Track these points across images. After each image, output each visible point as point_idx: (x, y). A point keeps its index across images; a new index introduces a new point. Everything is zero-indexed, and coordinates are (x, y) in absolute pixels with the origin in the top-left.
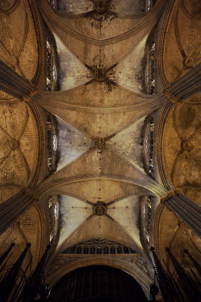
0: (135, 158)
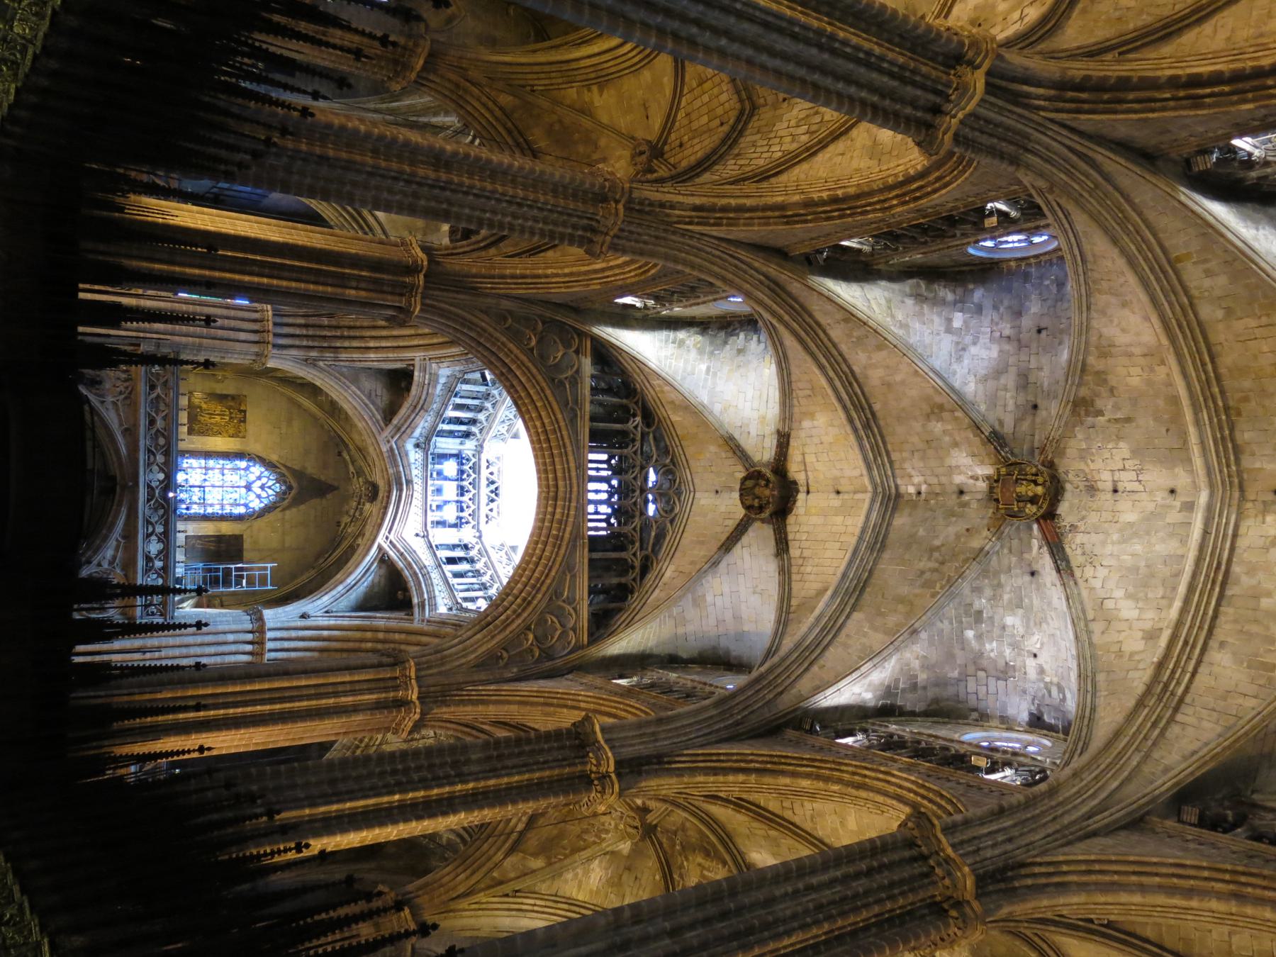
0: (955, 674)
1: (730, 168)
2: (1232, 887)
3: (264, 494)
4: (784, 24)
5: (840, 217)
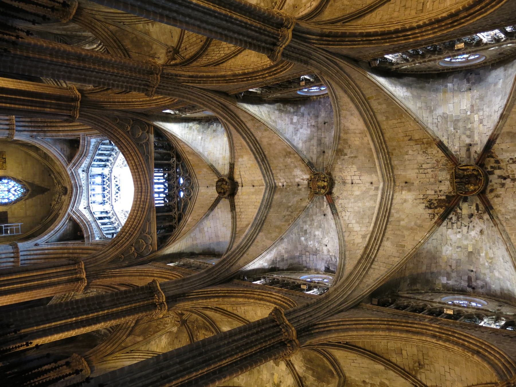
0: (298, 254)
1: (204, 60)
2: (387, 326)
3: (16, 194)
4: (211, 12)
5: (247, 80)
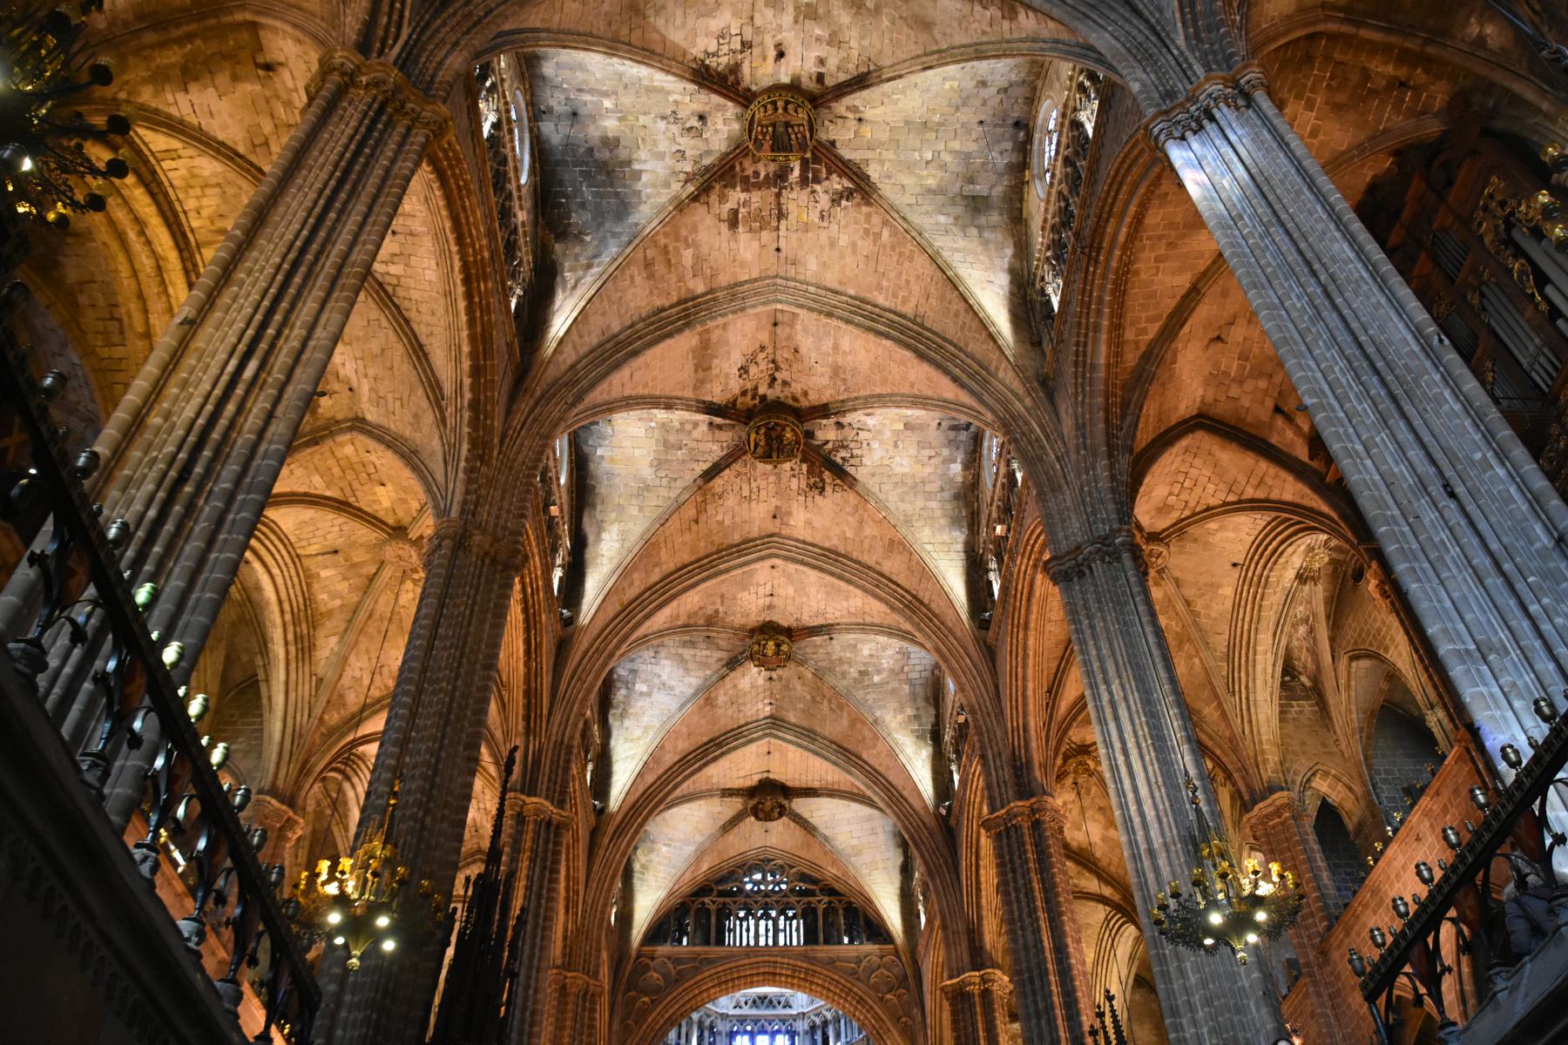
0: (907, 688)
